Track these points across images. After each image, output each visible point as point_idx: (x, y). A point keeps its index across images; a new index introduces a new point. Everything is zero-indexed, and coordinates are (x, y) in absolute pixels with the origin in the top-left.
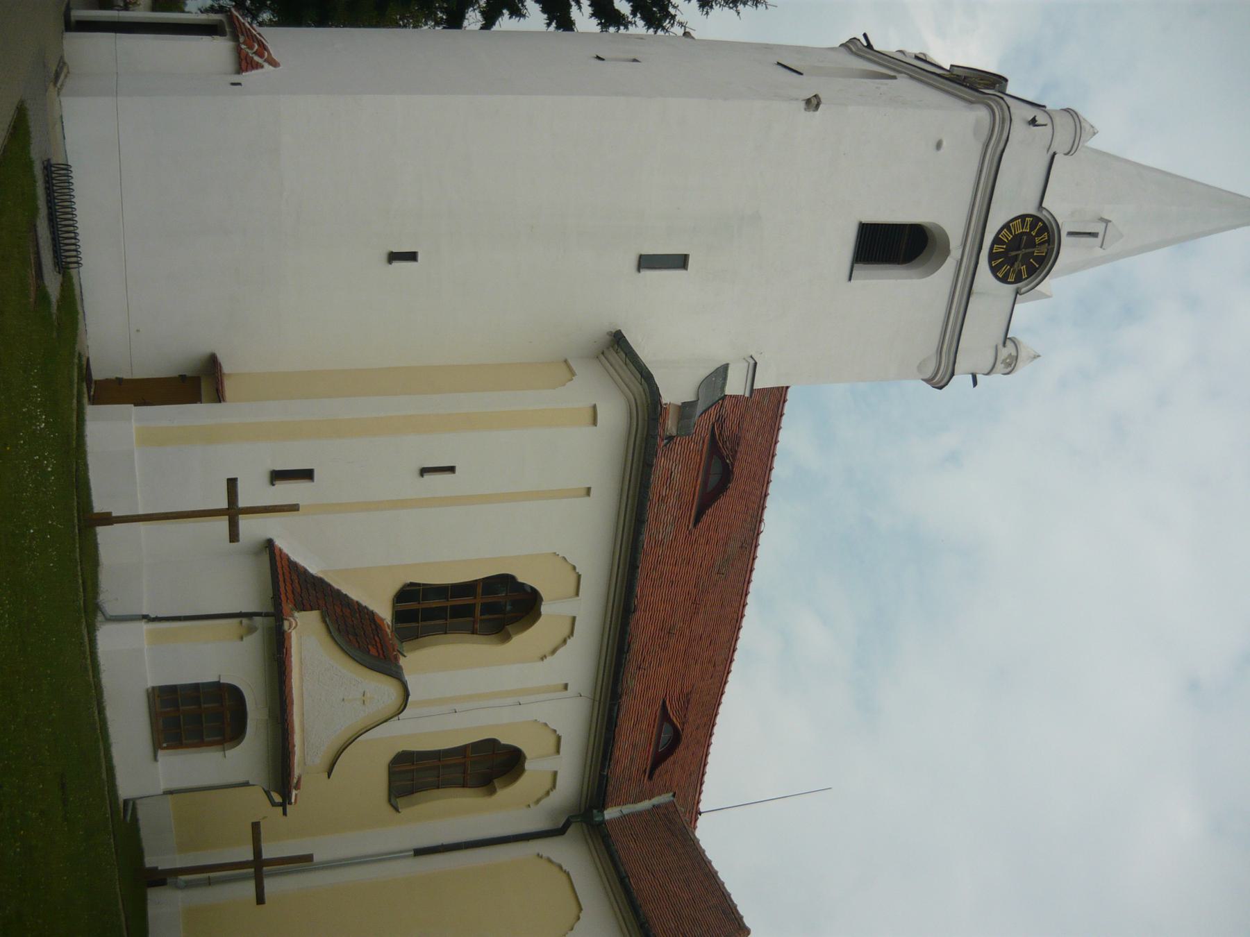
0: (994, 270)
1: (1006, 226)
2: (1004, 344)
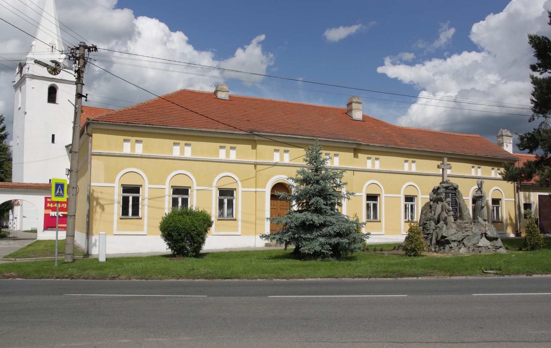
0: (58, 74)
1: (50, 72)
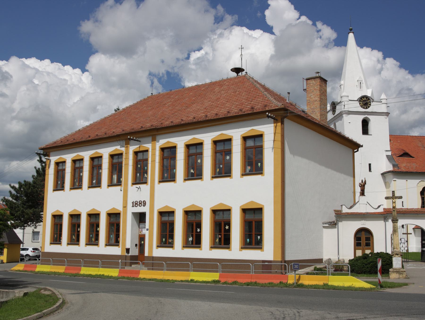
0: (369, 107)
1: (362, 106)
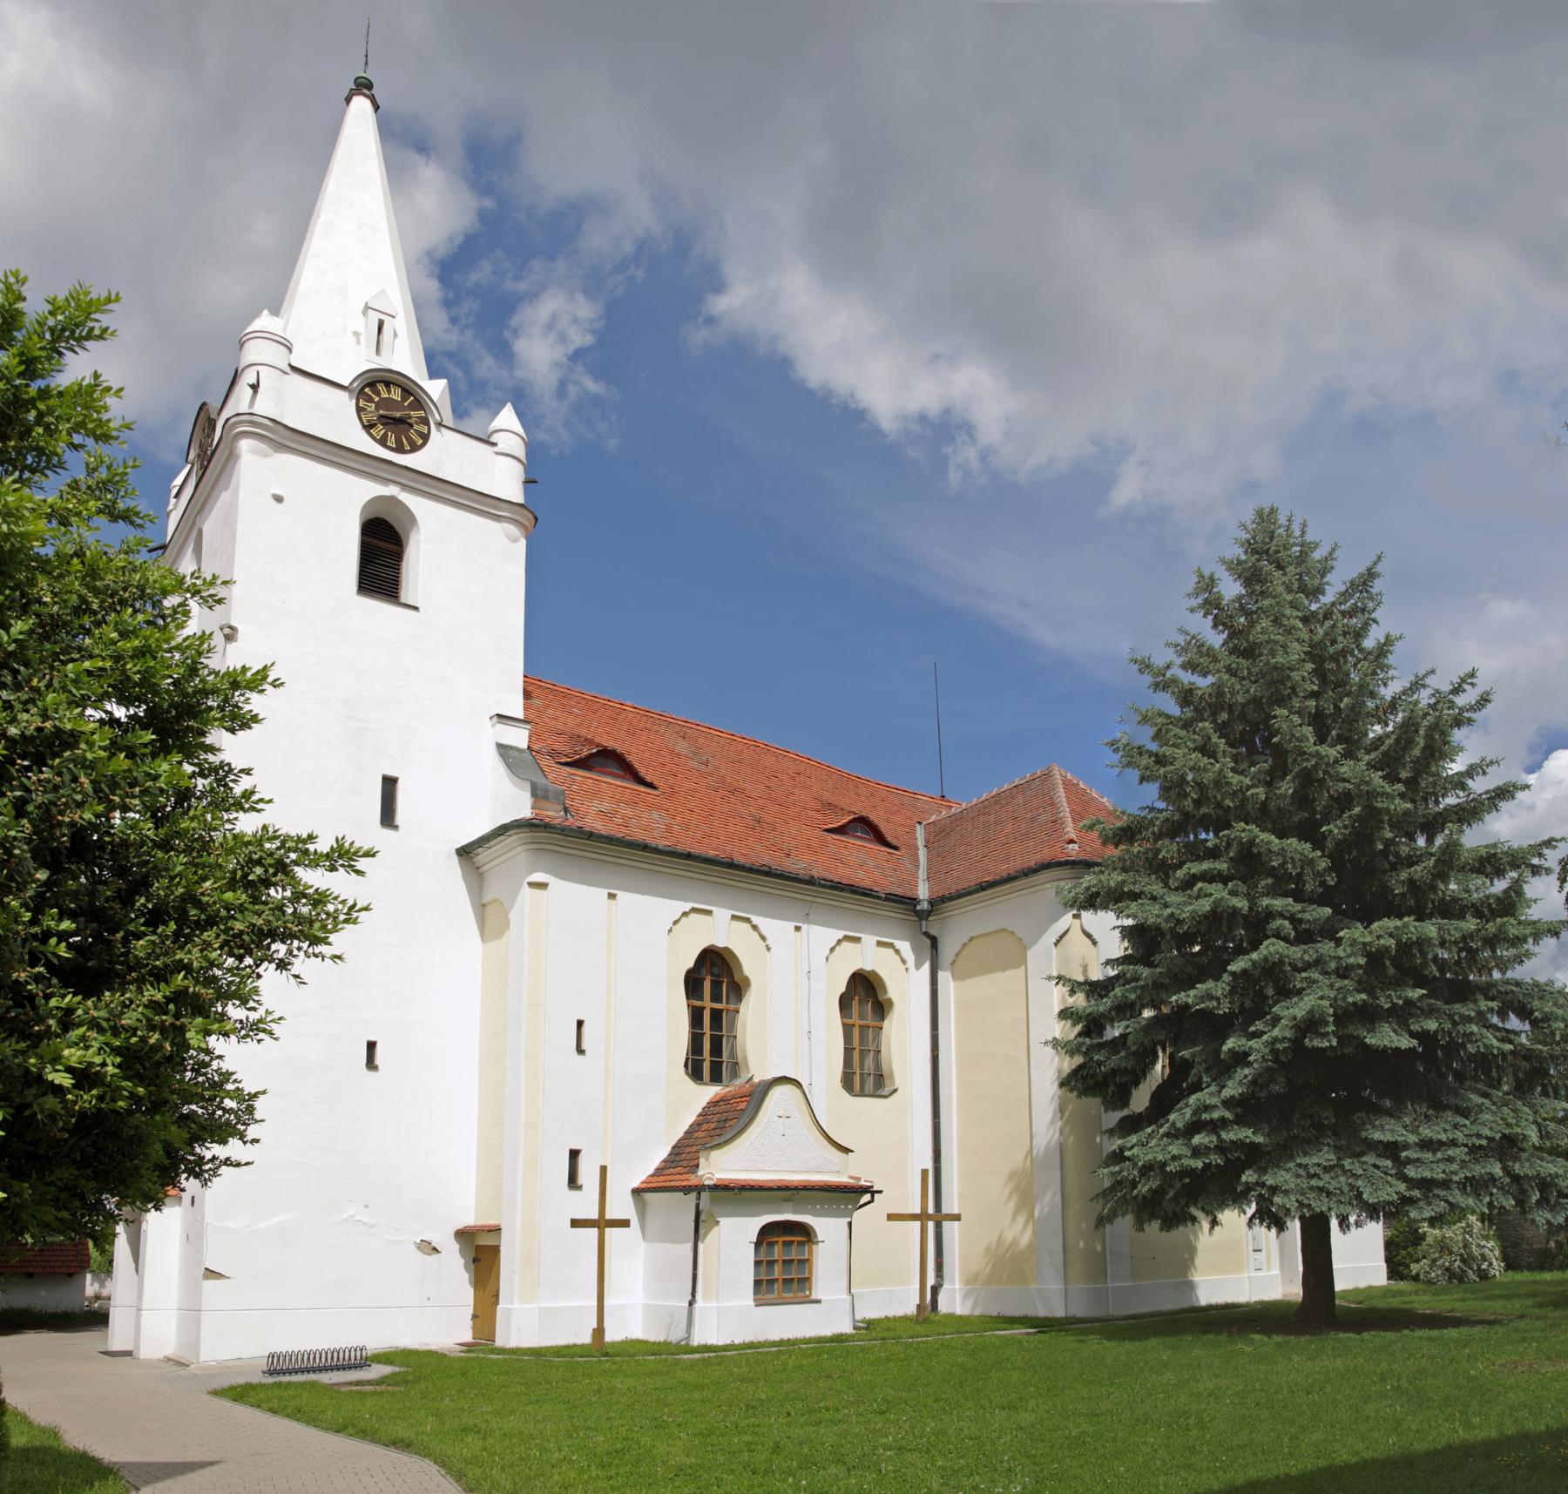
2: (494, 444)
